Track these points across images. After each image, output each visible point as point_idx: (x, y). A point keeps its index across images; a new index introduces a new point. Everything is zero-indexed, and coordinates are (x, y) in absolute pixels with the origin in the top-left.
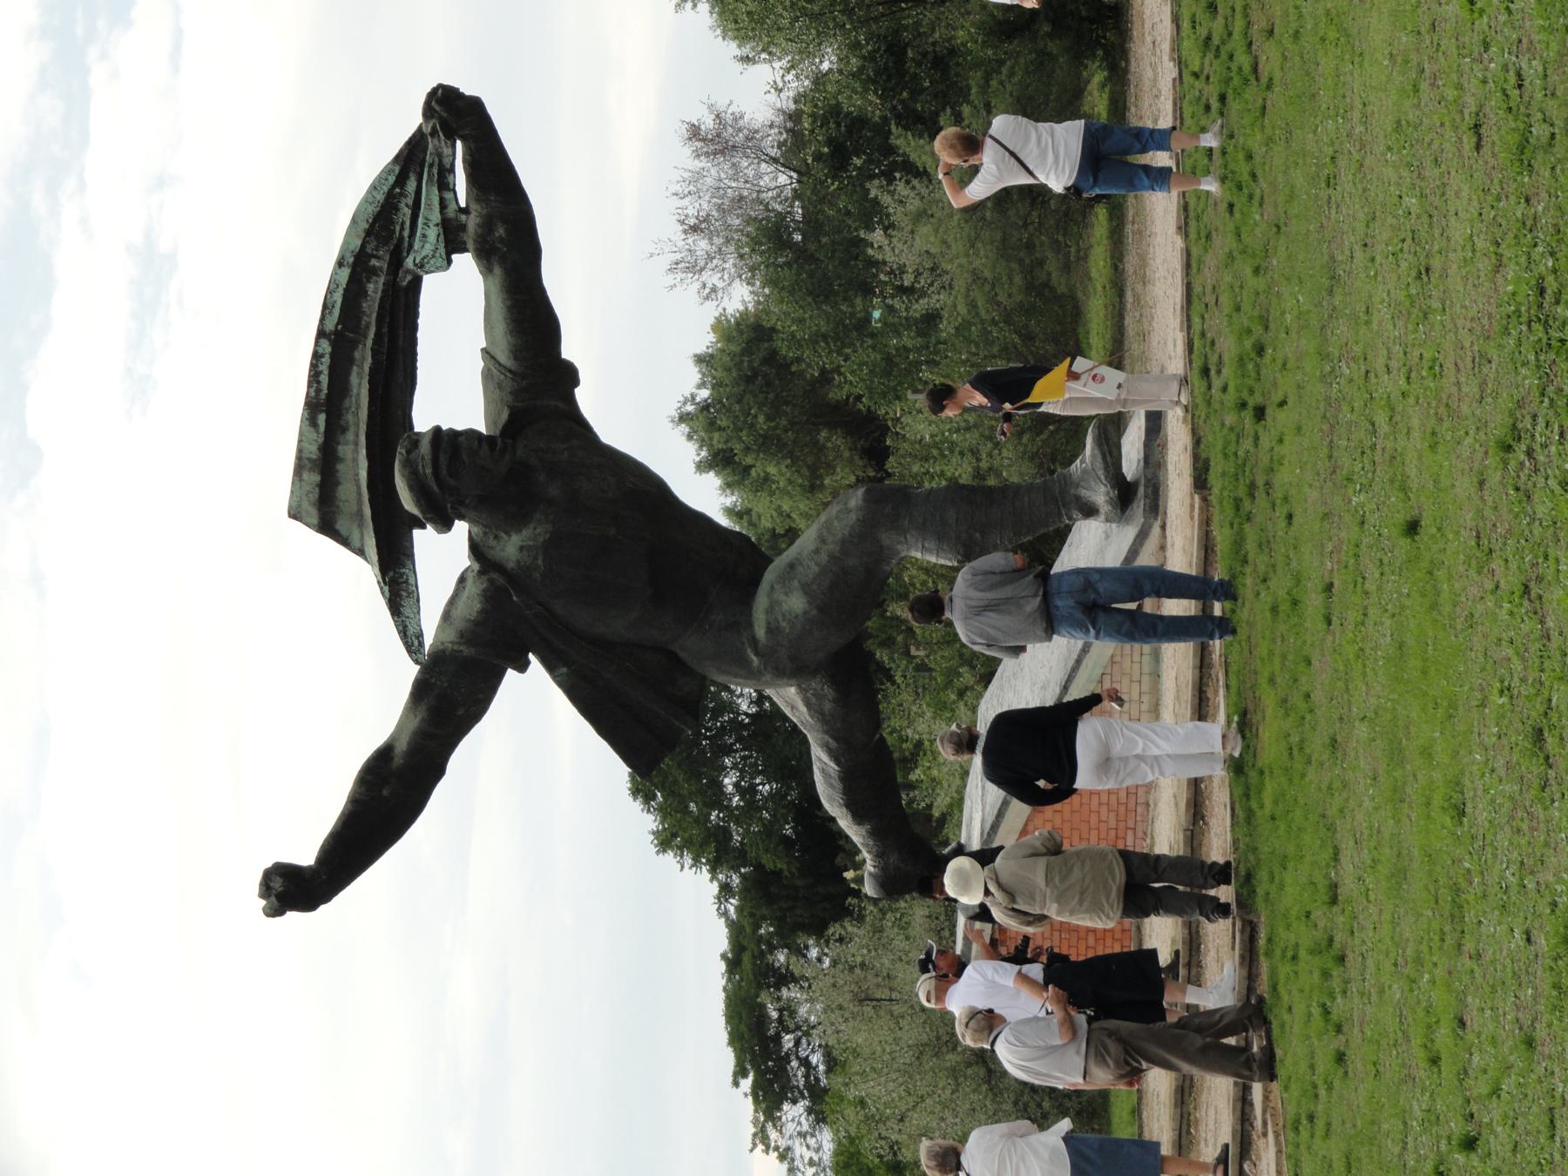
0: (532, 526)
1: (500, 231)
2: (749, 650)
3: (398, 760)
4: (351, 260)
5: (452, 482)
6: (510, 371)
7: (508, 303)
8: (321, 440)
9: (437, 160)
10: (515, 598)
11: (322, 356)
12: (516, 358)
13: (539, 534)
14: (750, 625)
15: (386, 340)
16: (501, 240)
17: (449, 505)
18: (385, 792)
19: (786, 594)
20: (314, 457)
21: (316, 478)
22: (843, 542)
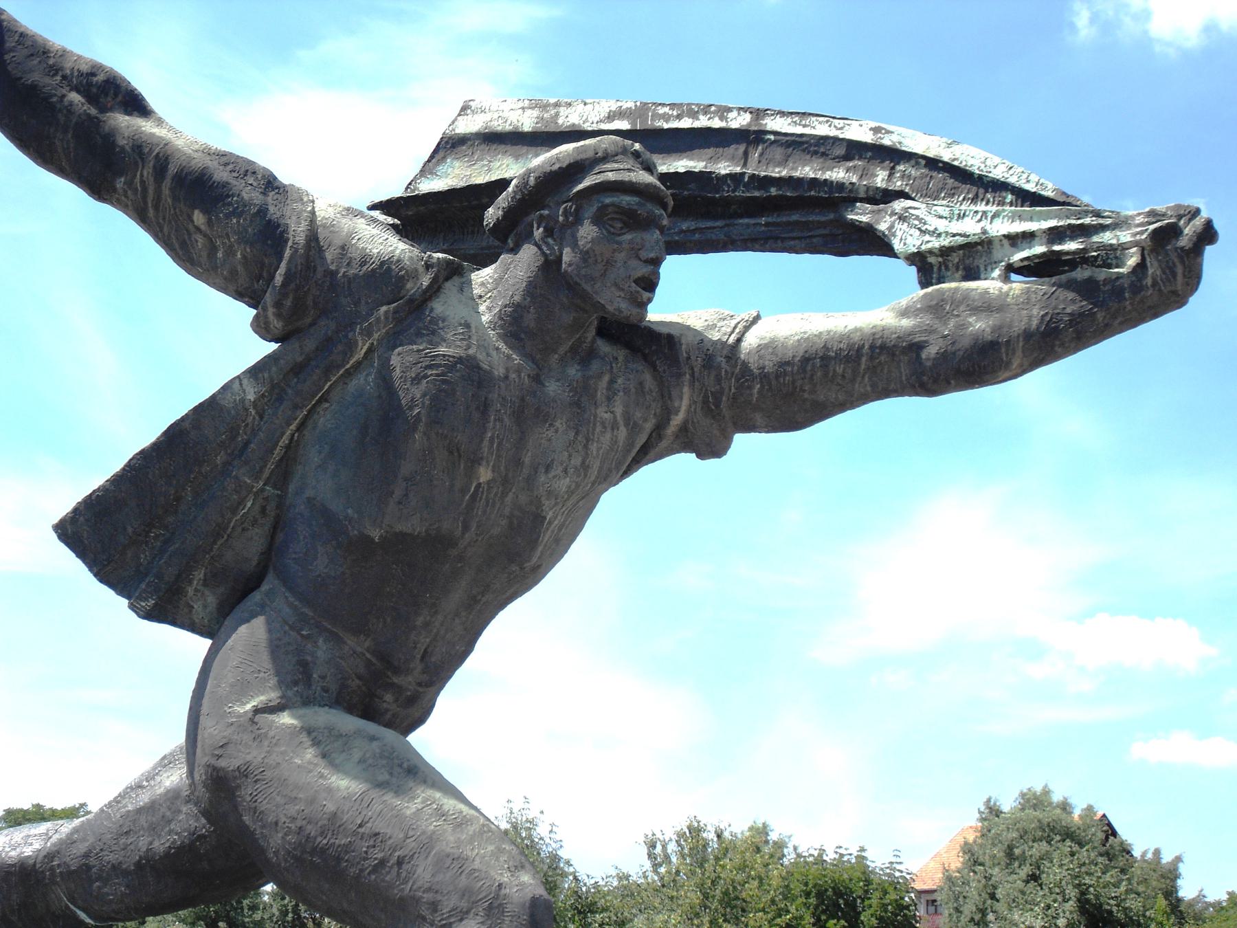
1: (979, 325)
2: (262, 698)
3: (123, 122)
4: (887, 141)
6: (739, 340)
7: (856, 337)
9: (1109, 221)
10: (384, 308)
11: (721, 118)
12: (760, 347)
13: (488, 355)
15: (757, 194)
16: (962, 326)
17: (546, 212)
19: (362, 761)
20: (560, 121)
21: (527, 128)
22: (459, 861)
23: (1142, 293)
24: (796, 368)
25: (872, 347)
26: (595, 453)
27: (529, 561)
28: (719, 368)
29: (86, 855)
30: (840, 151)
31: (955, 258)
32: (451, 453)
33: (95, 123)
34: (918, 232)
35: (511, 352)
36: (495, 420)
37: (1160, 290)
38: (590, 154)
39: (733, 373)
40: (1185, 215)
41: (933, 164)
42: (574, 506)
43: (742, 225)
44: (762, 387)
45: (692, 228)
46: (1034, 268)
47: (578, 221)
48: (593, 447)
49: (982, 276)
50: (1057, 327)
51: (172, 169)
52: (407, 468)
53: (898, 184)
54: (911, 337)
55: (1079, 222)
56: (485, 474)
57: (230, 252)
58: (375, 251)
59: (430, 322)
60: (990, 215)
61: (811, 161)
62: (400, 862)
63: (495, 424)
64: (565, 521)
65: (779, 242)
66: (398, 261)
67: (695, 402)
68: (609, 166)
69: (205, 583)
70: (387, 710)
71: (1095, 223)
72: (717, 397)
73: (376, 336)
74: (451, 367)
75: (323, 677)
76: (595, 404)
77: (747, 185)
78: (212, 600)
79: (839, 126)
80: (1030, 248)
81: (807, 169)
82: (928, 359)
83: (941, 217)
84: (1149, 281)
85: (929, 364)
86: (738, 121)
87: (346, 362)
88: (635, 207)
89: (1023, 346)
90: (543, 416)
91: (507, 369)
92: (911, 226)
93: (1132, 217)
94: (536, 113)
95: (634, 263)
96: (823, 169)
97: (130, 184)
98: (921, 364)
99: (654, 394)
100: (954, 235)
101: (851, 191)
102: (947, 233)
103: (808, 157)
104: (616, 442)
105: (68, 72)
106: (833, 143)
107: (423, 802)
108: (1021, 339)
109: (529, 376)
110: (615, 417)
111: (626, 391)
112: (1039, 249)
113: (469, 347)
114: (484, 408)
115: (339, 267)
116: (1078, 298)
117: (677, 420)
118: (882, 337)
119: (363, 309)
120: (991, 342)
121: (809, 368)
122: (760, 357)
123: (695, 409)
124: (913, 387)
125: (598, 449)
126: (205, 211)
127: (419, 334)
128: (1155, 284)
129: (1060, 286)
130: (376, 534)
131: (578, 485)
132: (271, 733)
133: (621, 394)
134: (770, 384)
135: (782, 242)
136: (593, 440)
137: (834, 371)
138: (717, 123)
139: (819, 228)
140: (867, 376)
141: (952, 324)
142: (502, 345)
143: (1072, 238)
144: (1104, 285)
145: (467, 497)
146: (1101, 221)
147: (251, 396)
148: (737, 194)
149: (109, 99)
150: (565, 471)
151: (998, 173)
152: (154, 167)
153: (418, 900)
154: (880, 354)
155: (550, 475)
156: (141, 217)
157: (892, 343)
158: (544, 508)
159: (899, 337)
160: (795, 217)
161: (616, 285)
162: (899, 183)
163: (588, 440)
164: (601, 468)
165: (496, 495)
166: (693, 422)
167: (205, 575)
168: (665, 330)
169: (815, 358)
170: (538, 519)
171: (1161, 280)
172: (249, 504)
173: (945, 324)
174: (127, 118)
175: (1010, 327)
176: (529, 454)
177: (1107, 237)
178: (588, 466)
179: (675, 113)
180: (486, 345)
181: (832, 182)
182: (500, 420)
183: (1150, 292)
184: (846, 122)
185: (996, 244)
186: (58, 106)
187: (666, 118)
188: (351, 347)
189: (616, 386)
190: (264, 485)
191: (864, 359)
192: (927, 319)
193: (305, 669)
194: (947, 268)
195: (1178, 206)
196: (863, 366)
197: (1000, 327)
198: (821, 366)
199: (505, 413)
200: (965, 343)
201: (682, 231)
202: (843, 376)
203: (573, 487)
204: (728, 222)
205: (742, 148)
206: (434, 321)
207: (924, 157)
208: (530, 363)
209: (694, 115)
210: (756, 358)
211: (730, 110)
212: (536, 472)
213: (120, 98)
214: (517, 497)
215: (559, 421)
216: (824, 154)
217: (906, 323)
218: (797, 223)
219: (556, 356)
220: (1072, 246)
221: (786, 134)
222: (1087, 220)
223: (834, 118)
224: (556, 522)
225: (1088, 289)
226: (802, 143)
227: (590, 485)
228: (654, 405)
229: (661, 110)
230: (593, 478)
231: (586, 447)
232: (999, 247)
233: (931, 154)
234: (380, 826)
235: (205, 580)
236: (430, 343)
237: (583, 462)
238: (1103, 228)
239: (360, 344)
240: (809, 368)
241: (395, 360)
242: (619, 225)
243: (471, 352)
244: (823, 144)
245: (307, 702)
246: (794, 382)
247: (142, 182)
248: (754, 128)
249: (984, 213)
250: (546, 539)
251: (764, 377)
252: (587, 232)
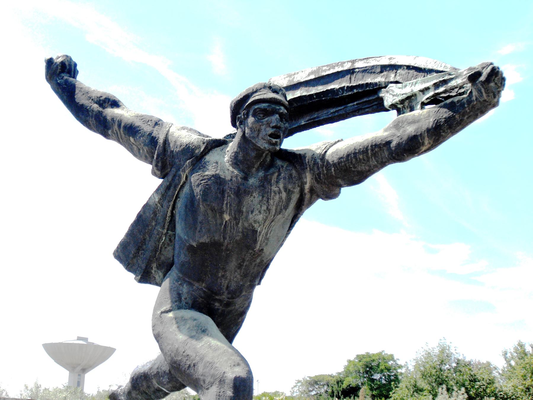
2: (165, 308)
5: (251, 112)
6: (326, 152)
8: (302, 80)
10: (188, 161)
11: (342, 66)
13: (224, 172)
15: (350, 93)
19: (189, 328)
23: (472, 104)
24: (345, 159)
25: (372, 146)
26: (272, 204)
27: (256, 248)
28: (318, 163)
29: (158, 368)
30: (379, 70)
31: (406, 104)
32: (212, 211)
33: (100, 113)
34: (391, 96)
35: (234, 170)
36: (227, 196)
37: (479, 101)
38: (251, 91)
39: (324, 165)
40: (485, 67)
41: (409, 67)
42: (270, 225)
43: (349, 106)
44: (334, 168)
45: (335, 111)
46: (434, 100)
47: (248, 117)
48: (271, 202)
49: (415, 109)
50: (440, 125)
51: (123, 124)
52: (200, 218)
53: (398, 78)
54: (387, 139)
55: (443, 79)
56: (227, 217)
57: (143, 150)
58: (185, 141)
59: (204, 163)
60: (414, 83)
61: (370, 76)
62: (194, 366)
63: (227, 198)
64: (268, 231)
65: (363, 110)
66: (192, 143)
67: (312, 179)
68: (257, 94)
69: (157, 268)
70: (218, 309)
71: (449, 78)
72: (319, 174)
73: (187, 172)
74: (209, 179)
75: (186, 299)
76: (271, 185)
77: (346, 91)
78: (161, 274)
79: (378, 60)
80: (428, 94)
81: (369, 79)
82: (393, 147)
83: (400, 88)
84: (474, 98)
85: (393, 149)
86: (347, 67)
87: (180, 182)
88: (266, 108)
89: (427, 135)
90: (248, 192)
91: (232, 177)
92: (390, 94)
93: (463, 72)
94: (288, 79)
95: (268, 129)
96: (374, 78)
97: (113, 132)
98: (391, 149)
99: (297, 178)
100: (403, 95)
101: (379, 85)
102: (400, 94)
103: (369, 75)
104: (282, 198)
105: (94, 98)
106: (376, 68)
107: (205, 342)
108: (426, 132)
109: (241, 178)
110: (280, 190)
111: (285, 178)
112: (431, 93)
113: (217, 170)
114: (223, 192)
115: (174, 149)
116: (448, 111)
117: (307, 187)
118: (375, 141)
119: (182, 163)
120: (414, 135)
121: (350, 158)
122: (332, 157)
123: (313, 181)
124: (391, 159)
125: (274, 203)
126: (133, 137)
127: (200, 169)
128: (476, 99)
129: (441, 107)
130: (194, 244)
131: (267, 217)
132: (165, 320)
133: (282, 179)
134: (337, 167)
135: (364, 110)
136: (270, 199)
137: (359, 158)
138: (340, 69)
139: (374, 102)
140: (373, 158)
141: (401, 131)
142: (231, 168)
143: (442, 86)
144: (458, 103)
145: (223, 227)
146: (451, 77)
147: (157, 200)
148: (344, 95)
149: (106, 104)
150: (260, 212)
151: (430, 66)
152: (118, 125)
153: (199, 379)
154: (375, 148)
155: (254, 215)
156: (119, 141)
157: (379, 143)
158: (255, 227)
159: (381, 140)
160: (365, 100)
161: (262, 138)
162: (398, 78)
163: (268, 199)
164: (276, 209)
165: (234, 224)
166: (315, 187)
167: (156, 265)
168: (298, 153)
169: (351, 154)
170: (255, 232)
171: (479, 96)
172: (164, 238)
173: (399, 131)
174: (111, 109)
175: (421, 128)
176: (245, 207)
177: (453, 83)
178: (270, 209)
179: (328, 68)
180: (224, 169)
181: (373, 83)
182: (230, 196)
183: (475, 103)
184: (381, 58)
185: (418, 94)
186: (89, 110)
187: (325, 71)
188: (180, 177)
189: (281, 177)
190: (167, 231)
191: (369, 151)
192: (393, 131)
193: (179, 295)
194: (405, 108)
195: (483, 64)
196: (370, 154)
197: (418, 129)
198: (354, 157)
199: (232, 193)
200: (405, 138)
201: (332, 113)
202: (364, 159)
203: (265, 217)
204: (345, 106)
205: (349, 76)
206: (205, 163)
207: (406, 66)
208: (242, 173)
209: (333, 67)
210: (331, 158)
211: (344, 63)
212: (248, 214)
213: (110, 103)
214: (244, 224)
215: (255, 193)
216: (374, 72)
217: (386, 134)
218: (366, 101)
219: (254, 169)
220: (441, 89)
221: (361, 68)
222: (446, 78)
223: (377, 57)
224: (263, 232)
225: (451, 107)
226: (367, 70)
227: (273, 216)
228: (297, 182)
229: (324, 68)
230: (273, 214)
231: (268, 202)
232: (419, 96)
233: (407, 64)
234: (188, 352)
235: (157, 267)
236: (203, 171)
237: (267, 208)
238: (452, 79)
239: (182, 175)
240: (350, 158)
241: (192, 180)
242: (262, 115)
243: (217, 172)
244: (373, 68)
245: (179, 308)
246: (345, 165)
247: (116, 130)
248: (352, 68)
249: (412, 83)
250: (260, 239)
251: (334, 165)
252: (251, 120)
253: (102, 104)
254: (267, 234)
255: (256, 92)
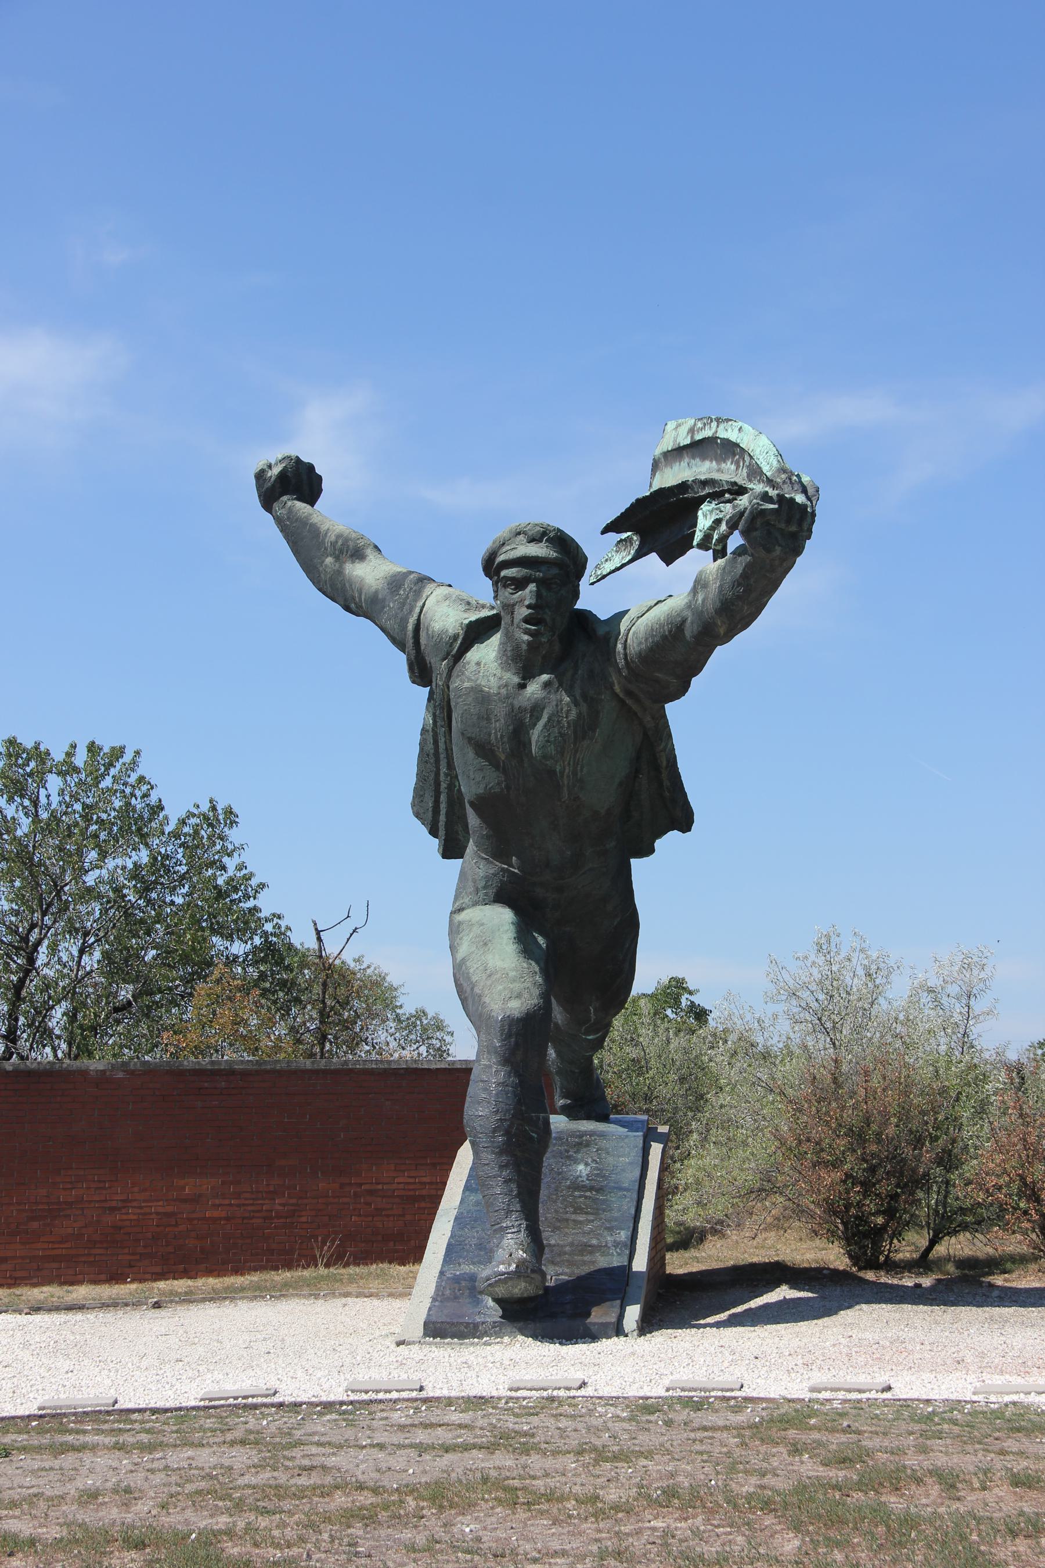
0: (499, 672)
13: (488, 681)
14: (475, 904)
18: (329, 560)
91: (499, 688)
224: (567, 771)
231: (559, 722)
250: (566, 782)
253: (339, 556)
254: (575, 773)
255: (504, 544)
